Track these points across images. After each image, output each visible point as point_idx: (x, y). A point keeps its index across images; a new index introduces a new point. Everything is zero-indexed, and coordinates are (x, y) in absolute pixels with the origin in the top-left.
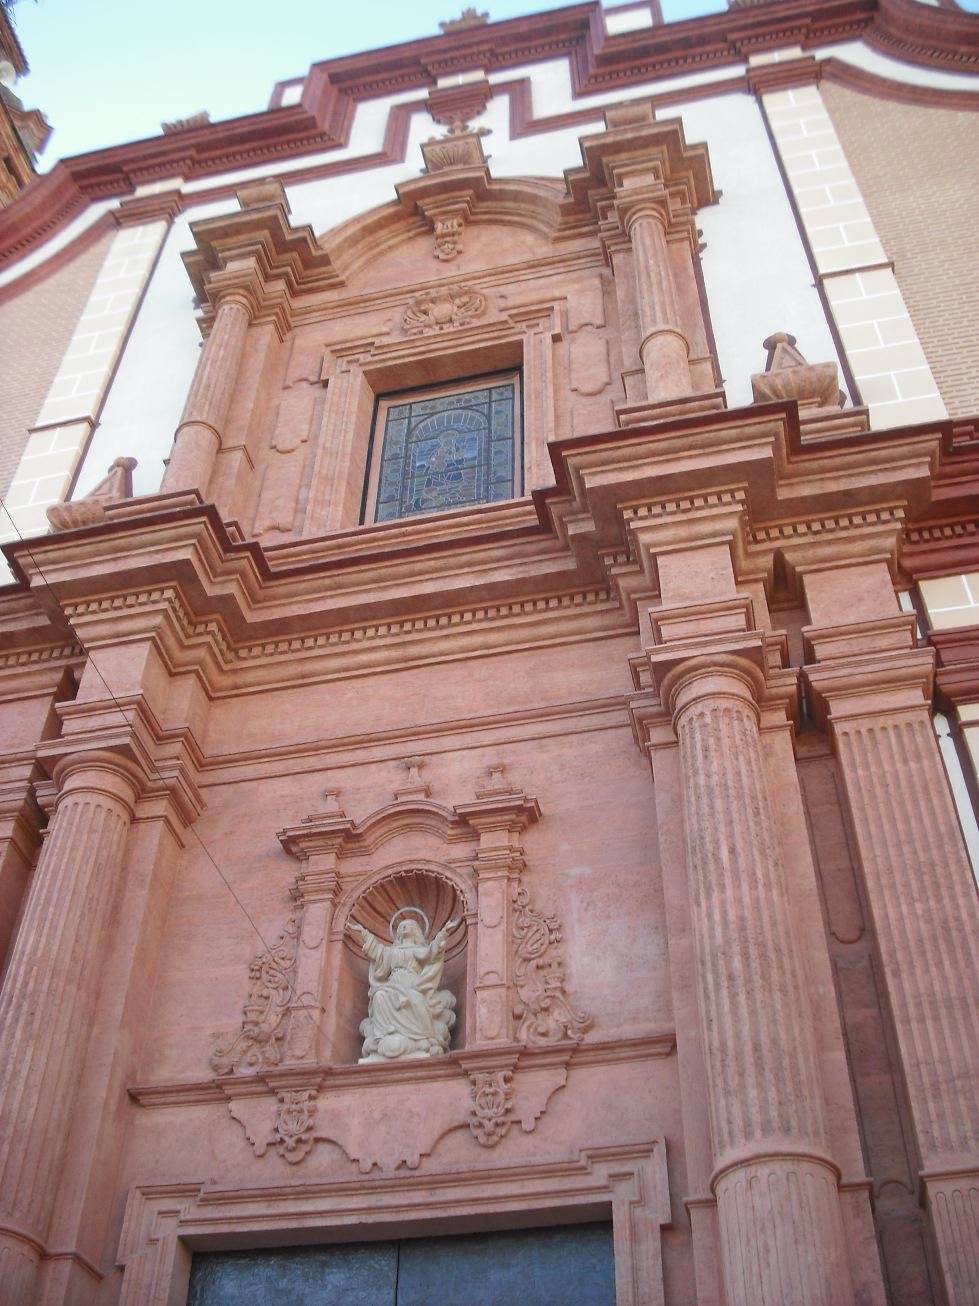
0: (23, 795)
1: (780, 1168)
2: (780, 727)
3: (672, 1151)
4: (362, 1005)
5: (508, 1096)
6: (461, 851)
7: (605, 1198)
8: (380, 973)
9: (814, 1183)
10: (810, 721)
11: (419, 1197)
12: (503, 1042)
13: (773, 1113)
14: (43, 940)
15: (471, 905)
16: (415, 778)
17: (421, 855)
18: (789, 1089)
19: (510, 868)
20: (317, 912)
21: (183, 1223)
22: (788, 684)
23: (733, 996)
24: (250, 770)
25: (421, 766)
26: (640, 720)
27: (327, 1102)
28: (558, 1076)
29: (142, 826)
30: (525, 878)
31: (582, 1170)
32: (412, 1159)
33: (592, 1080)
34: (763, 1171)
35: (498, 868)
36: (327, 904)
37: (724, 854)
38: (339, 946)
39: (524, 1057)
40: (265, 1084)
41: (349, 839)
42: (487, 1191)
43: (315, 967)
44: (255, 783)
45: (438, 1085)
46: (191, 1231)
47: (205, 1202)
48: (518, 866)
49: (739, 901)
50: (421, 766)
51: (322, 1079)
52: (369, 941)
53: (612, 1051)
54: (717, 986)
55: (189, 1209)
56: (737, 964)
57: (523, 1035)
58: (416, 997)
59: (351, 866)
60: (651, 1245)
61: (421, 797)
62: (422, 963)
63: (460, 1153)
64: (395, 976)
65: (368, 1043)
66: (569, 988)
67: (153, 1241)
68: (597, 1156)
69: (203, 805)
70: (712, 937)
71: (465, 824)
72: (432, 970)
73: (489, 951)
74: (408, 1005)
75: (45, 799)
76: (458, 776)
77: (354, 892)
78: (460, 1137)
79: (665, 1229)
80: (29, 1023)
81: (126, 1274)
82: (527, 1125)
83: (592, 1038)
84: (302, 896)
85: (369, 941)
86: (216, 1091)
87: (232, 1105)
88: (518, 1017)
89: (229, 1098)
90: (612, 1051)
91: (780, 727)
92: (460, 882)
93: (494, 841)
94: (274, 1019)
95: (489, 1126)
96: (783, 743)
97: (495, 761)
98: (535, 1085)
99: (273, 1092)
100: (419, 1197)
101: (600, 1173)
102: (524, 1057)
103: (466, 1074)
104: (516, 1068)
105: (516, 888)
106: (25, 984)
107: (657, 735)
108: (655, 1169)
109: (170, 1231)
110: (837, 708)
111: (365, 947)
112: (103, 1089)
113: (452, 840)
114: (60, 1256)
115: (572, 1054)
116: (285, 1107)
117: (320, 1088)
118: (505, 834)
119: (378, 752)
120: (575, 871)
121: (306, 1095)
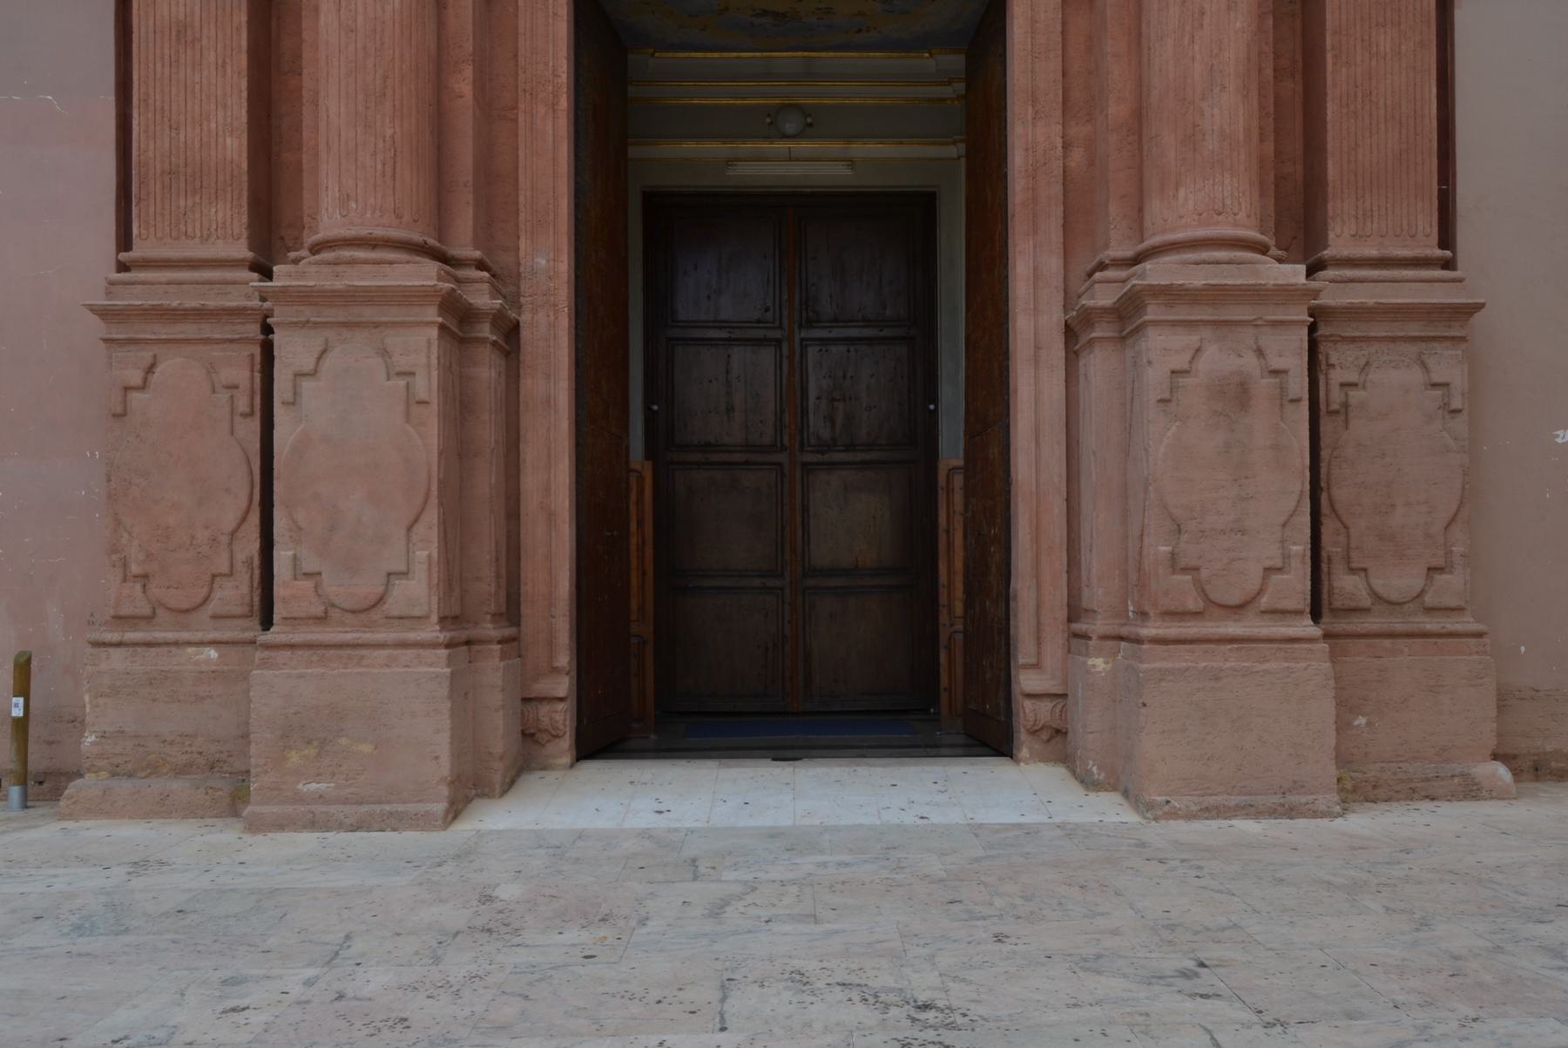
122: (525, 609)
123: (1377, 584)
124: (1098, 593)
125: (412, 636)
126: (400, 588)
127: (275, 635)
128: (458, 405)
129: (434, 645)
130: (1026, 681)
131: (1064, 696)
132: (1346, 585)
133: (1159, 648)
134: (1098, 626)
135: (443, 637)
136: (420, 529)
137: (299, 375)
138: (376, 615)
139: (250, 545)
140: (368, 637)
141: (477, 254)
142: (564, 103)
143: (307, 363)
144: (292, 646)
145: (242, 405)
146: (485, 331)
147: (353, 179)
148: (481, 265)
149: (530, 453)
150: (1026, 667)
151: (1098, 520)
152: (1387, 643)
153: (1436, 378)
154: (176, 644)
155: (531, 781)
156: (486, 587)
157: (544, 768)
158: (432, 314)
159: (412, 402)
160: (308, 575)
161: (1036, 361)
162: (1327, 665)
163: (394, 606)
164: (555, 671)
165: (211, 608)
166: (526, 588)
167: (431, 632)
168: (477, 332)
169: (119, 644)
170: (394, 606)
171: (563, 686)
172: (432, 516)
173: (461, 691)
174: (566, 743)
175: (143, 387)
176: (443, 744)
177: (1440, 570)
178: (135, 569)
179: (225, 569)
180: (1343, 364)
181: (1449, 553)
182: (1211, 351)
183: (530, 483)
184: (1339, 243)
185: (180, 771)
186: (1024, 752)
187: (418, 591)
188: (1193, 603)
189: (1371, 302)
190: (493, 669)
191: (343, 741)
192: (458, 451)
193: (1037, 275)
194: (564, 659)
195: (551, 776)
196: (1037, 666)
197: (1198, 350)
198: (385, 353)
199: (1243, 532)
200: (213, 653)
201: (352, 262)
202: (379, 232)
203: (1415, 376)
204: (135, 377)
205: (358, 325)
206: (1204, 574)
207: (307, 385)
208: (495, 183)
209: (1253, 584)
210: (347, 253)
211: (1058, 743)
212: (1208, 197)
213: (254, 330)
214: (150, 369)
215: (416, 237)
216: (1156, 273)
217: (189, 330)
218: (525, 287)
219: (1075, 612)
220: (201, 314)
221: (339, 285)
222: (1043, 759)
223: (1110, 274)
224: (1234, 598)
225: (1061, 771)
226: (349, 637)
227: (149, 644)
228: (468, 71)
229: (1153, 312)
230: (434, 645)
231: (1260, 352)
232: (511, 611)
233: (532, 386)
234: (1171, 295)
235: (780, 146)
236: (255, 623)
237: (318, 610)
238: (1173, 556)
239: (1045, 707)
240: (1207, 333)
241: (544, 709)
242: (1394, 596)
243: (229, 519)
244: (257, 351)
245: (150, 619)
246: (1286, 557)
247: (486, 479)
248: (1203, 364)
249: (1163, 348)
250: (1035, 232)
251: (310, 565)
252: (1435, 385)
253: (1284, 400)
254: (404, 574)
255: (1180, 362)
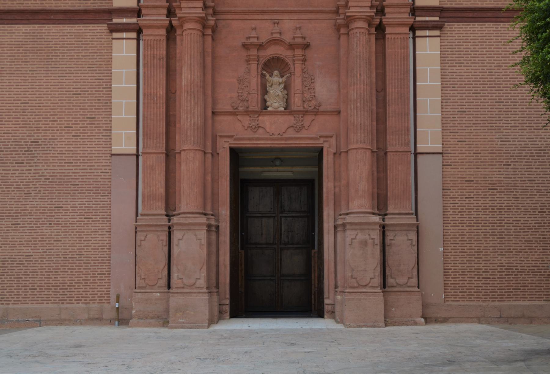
0: (168, 22)
1: (363, 151)
2: (373, 34)
3: (337, 137)
4: (265, 91)
5: (302, 121)
6: (289, 53)
7: (322, 145)
8: (270, 85)
9: (368, 153)
10: (380, 29)
11: (283, 142)
12: (301, 108)
13: (363, 139)
14: (193, 77)
15: (292, 69)
16: (277, 29)
17: (279, 52)
18: (366, 134)
19: (302, 61)
20: (254, 66)
21: (230, 144)
22: (377, 21)
23: (357, 112)
24: (229, 16)
25: (278, 24)
26: (339, 25)
27: (261, 118)
28: (313, 117)
29: (205, 37)
30: (306, 63)
31: (318, 139)
32: (281, 133)
33: (321, 118)
34: (360, 151)
35: (299, 60)
36: (256, 65)
37: (359, 76)
38: (259, 76)
39: (305, 113)
40: (247, 113)
41: (260, 47)
42: (297, 142)
43: (255, 82)
44: (231, 21)
45: (286, 116)
46: (232, 146)
47: (235, 139)
48: (304, 60)
49: (360, 88)
50: (278, 24)
51: (259, 113)
52: (268, 76)
53: (325, 113)
54: (354, 108)
55: (231, 141)
56: (359, 104)
57: (305, 106)
58: (280, 93)
59: (261, 53)
60: (331, 156)
61: (278, 35)
62: (280, 84)
63: (291, 133)
64: (273, 86)
65: (268, 104)
66: (316, 95)
67: (224, 148)
68: (321, 136)
69: (217, 26)
70: (354, 96)
71: (291, 47)
72: (282, 86)
73: (297, 83)
74: (278, 95)
75: (175, 24)
76: (288, 27)
77: (263, 61)
78: (292, 129)
79: (334, 154)
80: (194, 99)
81: (220, 155)
82: (306, 128)
83: (321, 109)
84: (249, 61)
85: (268, 76)
86: (234, 113)
87: (238, 117)
88: (304, 101)
89: (237, 115)
90: (325, 113)
91: (373, 34)
92: (289, 61)
93: (298, 52)
94: (245, 95)
95: (298, 127)
96: (373, 38)
97: (298, 26)
98: (308, 119)
99: (248, 115)
100: (283, 142)
101: (321, 141)
102: (305, 113)
103: (293, 114)
104: (304, 115)
105: (304, 66)
106: (191, 89)
107: (343, 31)
108: (333, 141)
109: (227, 146)
110: (388, 30)
111: (267, 78)
112: (209, 114)
113: (287, 49)
114: (208, 153)
115: (316, 112)
116: (251, 119)
117: (259, 115)
118: (301, 50)
119: (266, 17)
120: (318, 63)
121: (256, 116)
122: (220, 286)
123: (397, 281)
124: (339, 283)
125: (201, 291)
126: (199, 281)
127: (171, 290)
128: (209, 244)
129: (205, 293)
130: (326, 301)
131: (334, 304)
132: (390, 281)
133: (349, 294)
134: (339, 289)
135: (207, 291)
136: (202, 270)
137: (179, 240)
138: (193, 287)
139: (166, 272)
140: (192, 291)
141: (212, 213)
142: (228, 179)
143: (180, 237)
144: (177, 293)
145: (164, 244)
146: (214, 229)
147: (188, 200)
148: (212, 215)
149: (221, 252)
150: (326, 298)
151: (339, 267)
152: (399, 293)
153: (410, 238)
154: (151, 292)
155: (221, 321)
156: (214, 281)
157: (224, 319)
158: (205, 228)
159: (201, 245)
160: (181, 279)
161: (328, 233)
162: (382, 298)
163: (197, 285)
164: (226, 298)
165: (158, 285)
166: (220, 281)
167: (204, 290)
168: (213, 229)
169: (140, 292)
170: (197, 285)
171: (228, 302)
172: (205, 267)
173: (210, 302)
174: (228, 314)
175: (144, 240)
176: (207, 312)
177: (411, 278)
178: (143, 277)
179: (160, 277)
180: (390, 236)
181: (412, 275)
182: (360, 235)
183: (221, 259)
184: (391, 210)
185: (152, 318)
186: (326, 316)
187: (202, 282)
188: (356, 285)
189: (395, 223)
190: (215, 298)
191: (188, 311)
192: (209, 254)
193: (328, 215)
194: (228, 296)
195: (225, 321)
196: (328, 298)
197: (357, 235)
198: (196, 235)
199: (366, 271)
200: (159, 294)
201: (189, 217)
202: (194, 211)
203: (405, 238)
204: (143, 238)
205: (191, 230)
206: (358, 279)
207: (180, 241)
208: (215, 196)
209: (368, 281)
210: (188, 215)
211: (332, 314)
212: (360, 203)
213: (167, 229)
214: (146, 237)
215: (201, 211)
216: (349, 219)
217: (153, 229)
218: (220, 218)
219: (336, 287)
220: (156, 226)
221: (187, 222)
222: (330, 318)
223: (342, 217)
224: (364, 284)
225: (333, 320)
226: (189, 291)
227: (146, 292)
228: (210, 175)
229: (348, 227)
230: (205, 293)
231: (369, 235)
232: (217, 287)
233: (222, 238)
234: (351, 224)
235: (275, 168)
236: (166, 288)
237: (182, 286)
238: (352, 276)
239: (330, 307)
240: (359, 231)
241: (224, 307)
242: (401, 284)
243: (162, 267)
244: (167, 233)
245: (145, 287)
246: (374, 276)
247: (214, 258)
248: (358, 237)
249: (350, 234)
250: (328, 206)
251: (181, 277)
252: (410, 240)
253: (374, 244)
254: (199, 279)
255: (353, 237)
